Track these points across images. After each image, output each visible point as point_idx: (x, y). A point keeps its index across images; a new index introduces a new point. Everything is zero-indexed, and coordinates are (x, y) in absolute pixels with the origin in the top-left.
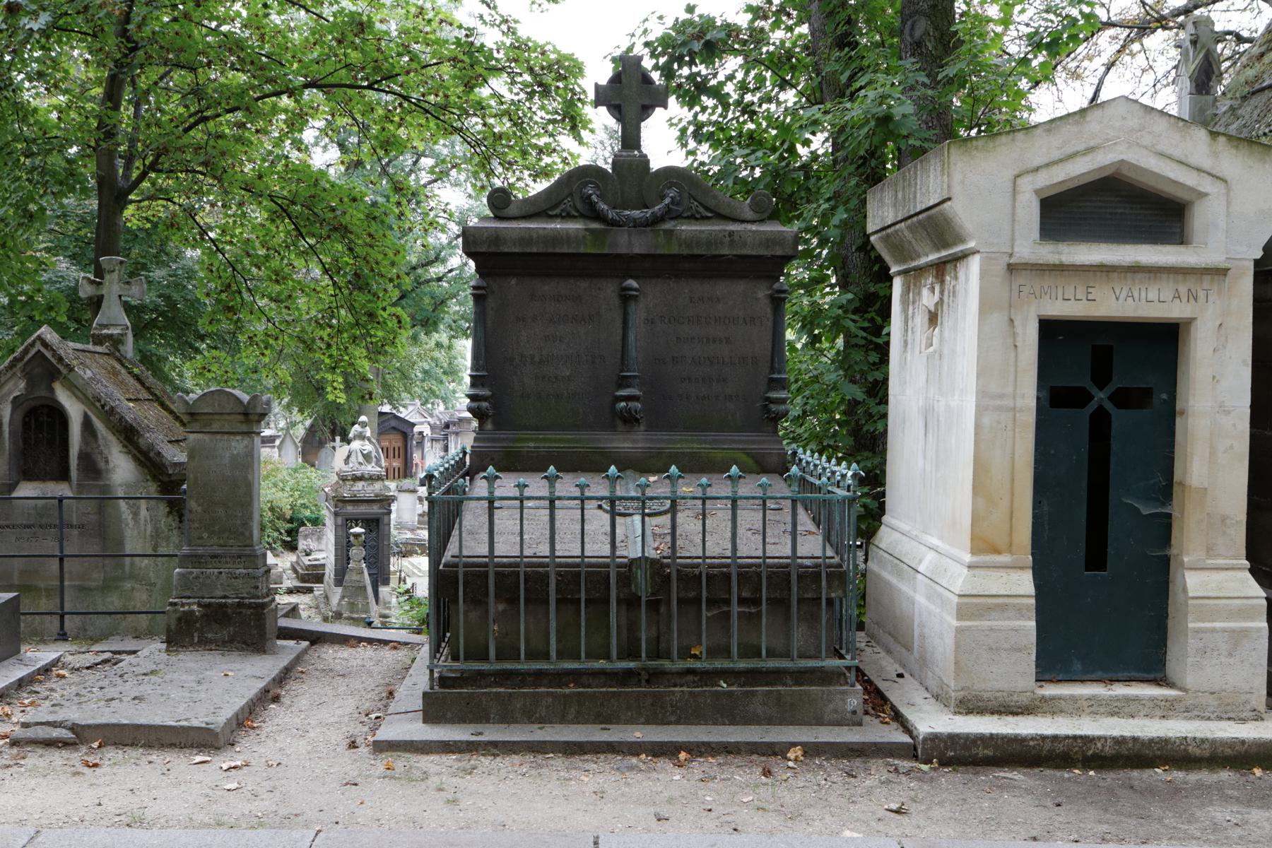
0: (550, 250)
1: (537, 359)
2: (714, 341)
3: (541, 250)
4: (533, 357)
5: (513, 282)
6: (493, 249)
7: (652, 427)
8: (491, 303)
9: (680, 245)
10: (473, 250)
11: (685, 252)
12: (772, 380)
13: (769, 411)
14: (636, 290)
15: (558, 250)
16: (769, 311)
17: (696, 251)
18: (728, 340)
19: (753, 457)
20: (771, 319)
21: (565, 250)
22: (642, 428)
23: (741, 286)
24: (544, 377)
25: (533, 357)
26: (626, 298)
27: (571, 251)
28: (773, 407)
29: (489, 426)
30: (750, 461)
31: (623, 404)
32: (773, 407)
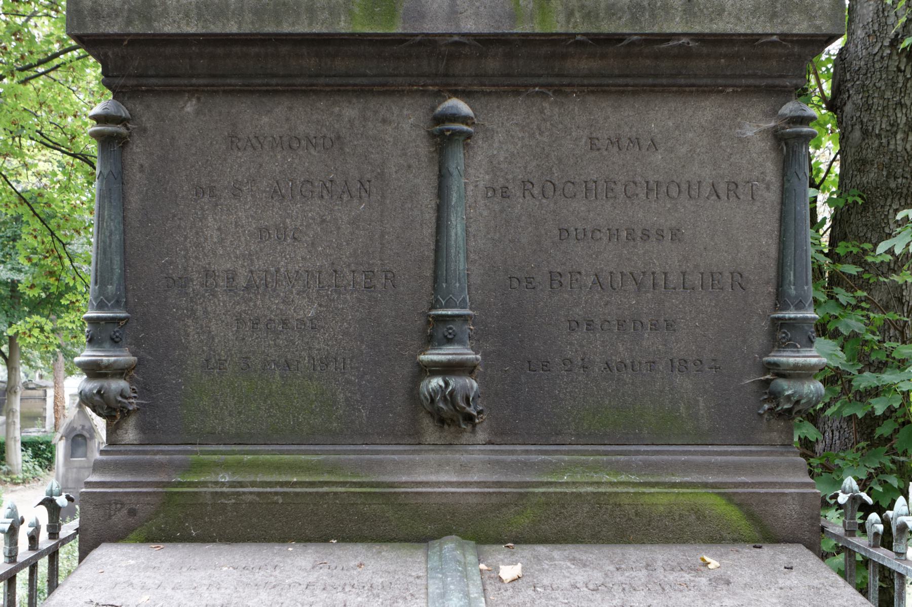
0: (270, 29)
1: (242, 282)
2: (646, 236)
3: (247, 29)
4: (231, 277)
5: (190, 107)
6: (137, 28)
7: (503, 434)
8: (138, 151)
9: (570, 14)
10: (91, 29)
11: (580, 27)
12: (779, 325)
13: (775, 396)
14: (465, 120)
15: (286, 28)
16: (770, 169)
17: (608, 27)
18: (676, 234)
19: (740, 505)
20: (776, 186)
21: (302, 28)
22: (481, 436)
23: (705, 112)
24: (256, 322)
25: (231, 277)
26: (445, 137)
27: (317, 29)
28: (788, 388)
29: (130, 434)
30: (733, 514)
31: (436, 382)
32: (788, 388)
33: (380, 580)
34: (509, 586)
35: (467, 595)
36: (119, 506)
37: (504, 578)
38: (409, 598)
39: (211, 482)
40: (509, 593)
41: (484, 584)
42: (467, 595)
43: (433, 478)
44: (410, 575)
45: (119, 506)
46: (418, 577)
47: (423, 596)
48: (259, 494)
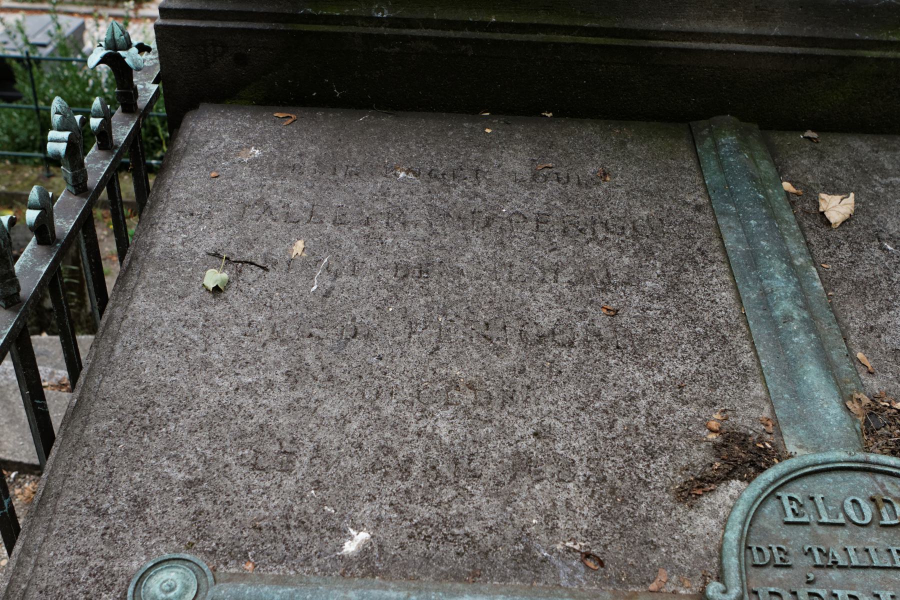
33: (644, 213)
34: (840, 235)
35: (788, 259)
36: (219, 49)
37: (832, 221)
38: (699, 258)
39: (361, 17)
40: (845, 253)
41: (802, 230)
42: (788, 259)
43: (710, 26)
44: (686, 204)
45: (219, 49)
46: (698, 208)
47: (719, 255)
48: (437, 40)
